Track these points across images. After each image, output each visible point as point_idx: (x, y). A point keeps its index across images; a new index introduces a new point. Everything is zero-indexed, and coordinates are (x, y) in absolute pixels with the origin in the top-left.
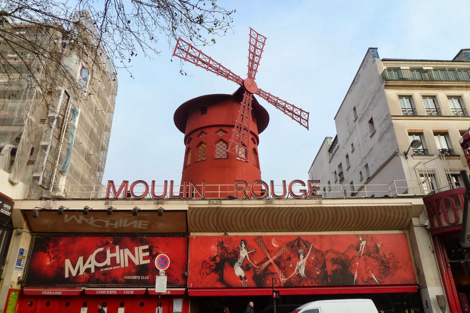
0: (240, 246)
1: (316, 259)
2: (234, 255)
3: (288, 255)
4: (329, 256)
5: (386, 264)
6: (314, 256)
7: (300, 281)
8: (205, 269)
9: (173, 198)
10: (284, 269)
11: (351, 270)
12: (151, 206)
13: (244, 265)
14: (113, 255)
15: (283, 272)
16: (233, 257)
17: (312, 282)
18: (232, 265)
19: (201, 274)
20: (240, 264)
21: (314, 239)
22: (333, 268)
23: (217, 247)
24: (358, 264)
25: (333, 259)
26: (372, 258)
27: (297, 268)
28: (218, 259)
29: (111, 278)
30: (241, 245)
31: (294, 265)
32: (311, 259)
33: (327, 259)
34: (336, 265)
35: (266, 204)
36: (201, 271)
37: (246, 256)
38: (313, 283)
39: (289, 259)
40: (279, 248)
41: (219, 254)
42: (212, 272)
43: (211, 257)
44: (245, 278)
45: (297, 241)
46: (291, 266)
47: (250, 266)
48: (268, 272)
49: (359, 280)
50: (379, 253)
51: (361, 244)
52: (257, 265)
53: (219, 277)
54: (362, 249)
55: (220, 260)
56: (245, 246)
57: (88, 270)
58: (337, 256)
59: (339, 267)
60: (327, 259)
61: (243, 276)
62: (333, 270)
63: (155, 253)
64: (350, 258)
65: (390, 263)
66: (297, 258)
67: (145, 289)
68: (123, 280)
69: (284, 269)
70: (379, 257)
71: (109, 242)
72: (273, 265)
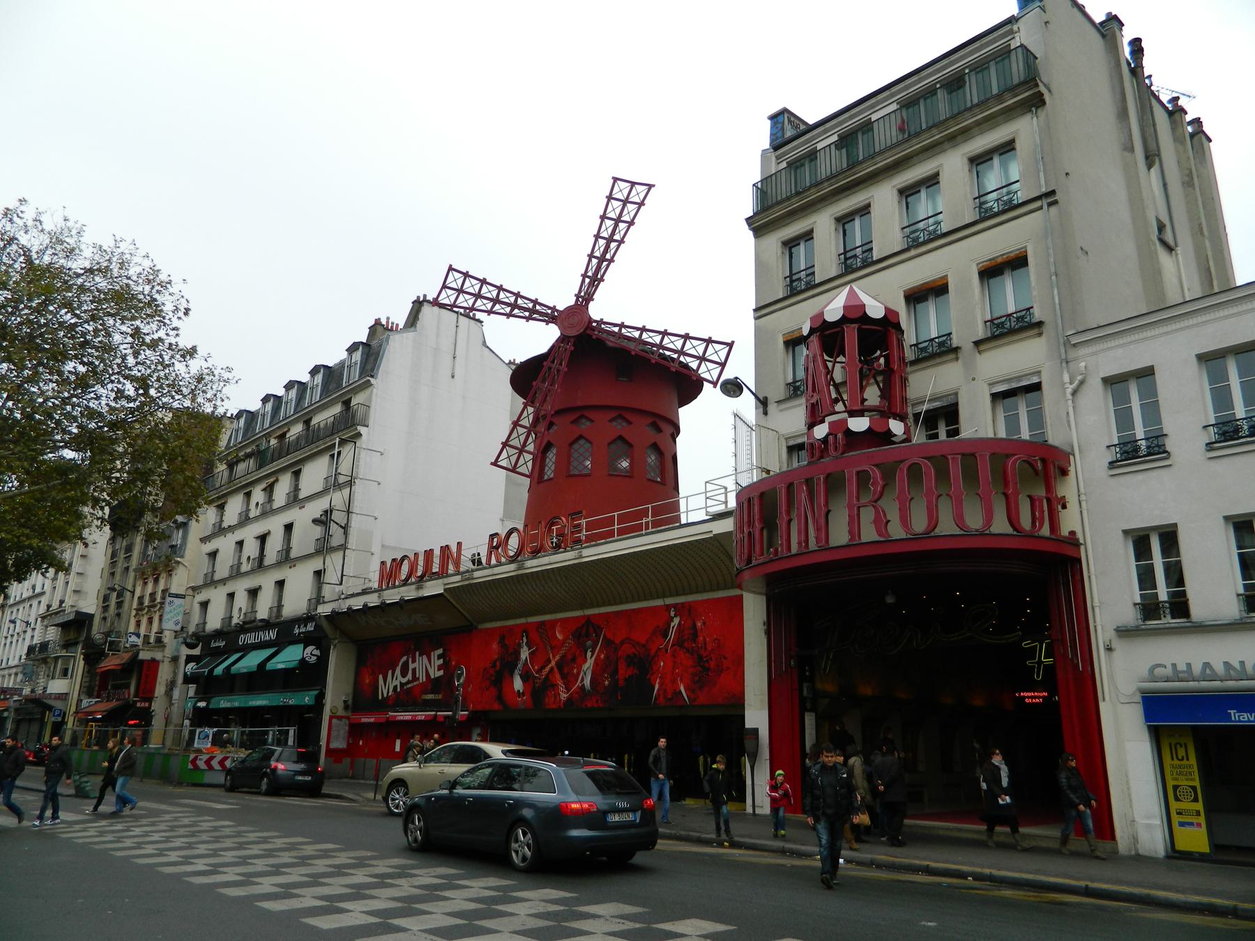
1: (607, 657)
15: (564, 683)
24: (662, 664)
27: (582, 673)
35: (519, 569)
39: (574, 660)
40: (564, 642)
44: (523, 694)
46: (575, 671)
51: (672, 624)
54: (672, 635)
57: (395, 687)
59: (635, 671)
61: (521, 691)
64: (653, 653)
65: (711, 659)
67: (433, 713)
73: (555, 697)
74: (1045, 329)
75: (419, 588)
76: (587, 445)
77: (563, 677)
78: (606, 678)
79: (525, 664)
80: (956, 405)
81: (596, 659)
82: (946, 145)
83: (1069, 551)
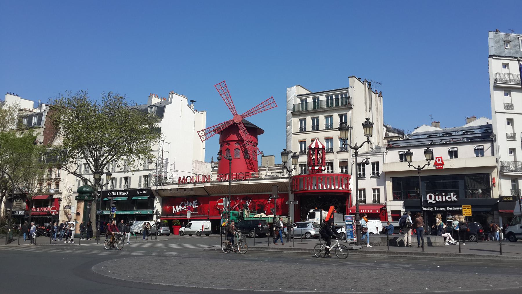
9: (200, 183)
12: (191, 186)
14: (186, 204)
57: (180, 210)
64: (265, 204)
74: (349, 152)
75: (194, 185)
80: (333, 162)
82: (335, 110)
83: (350, 192)
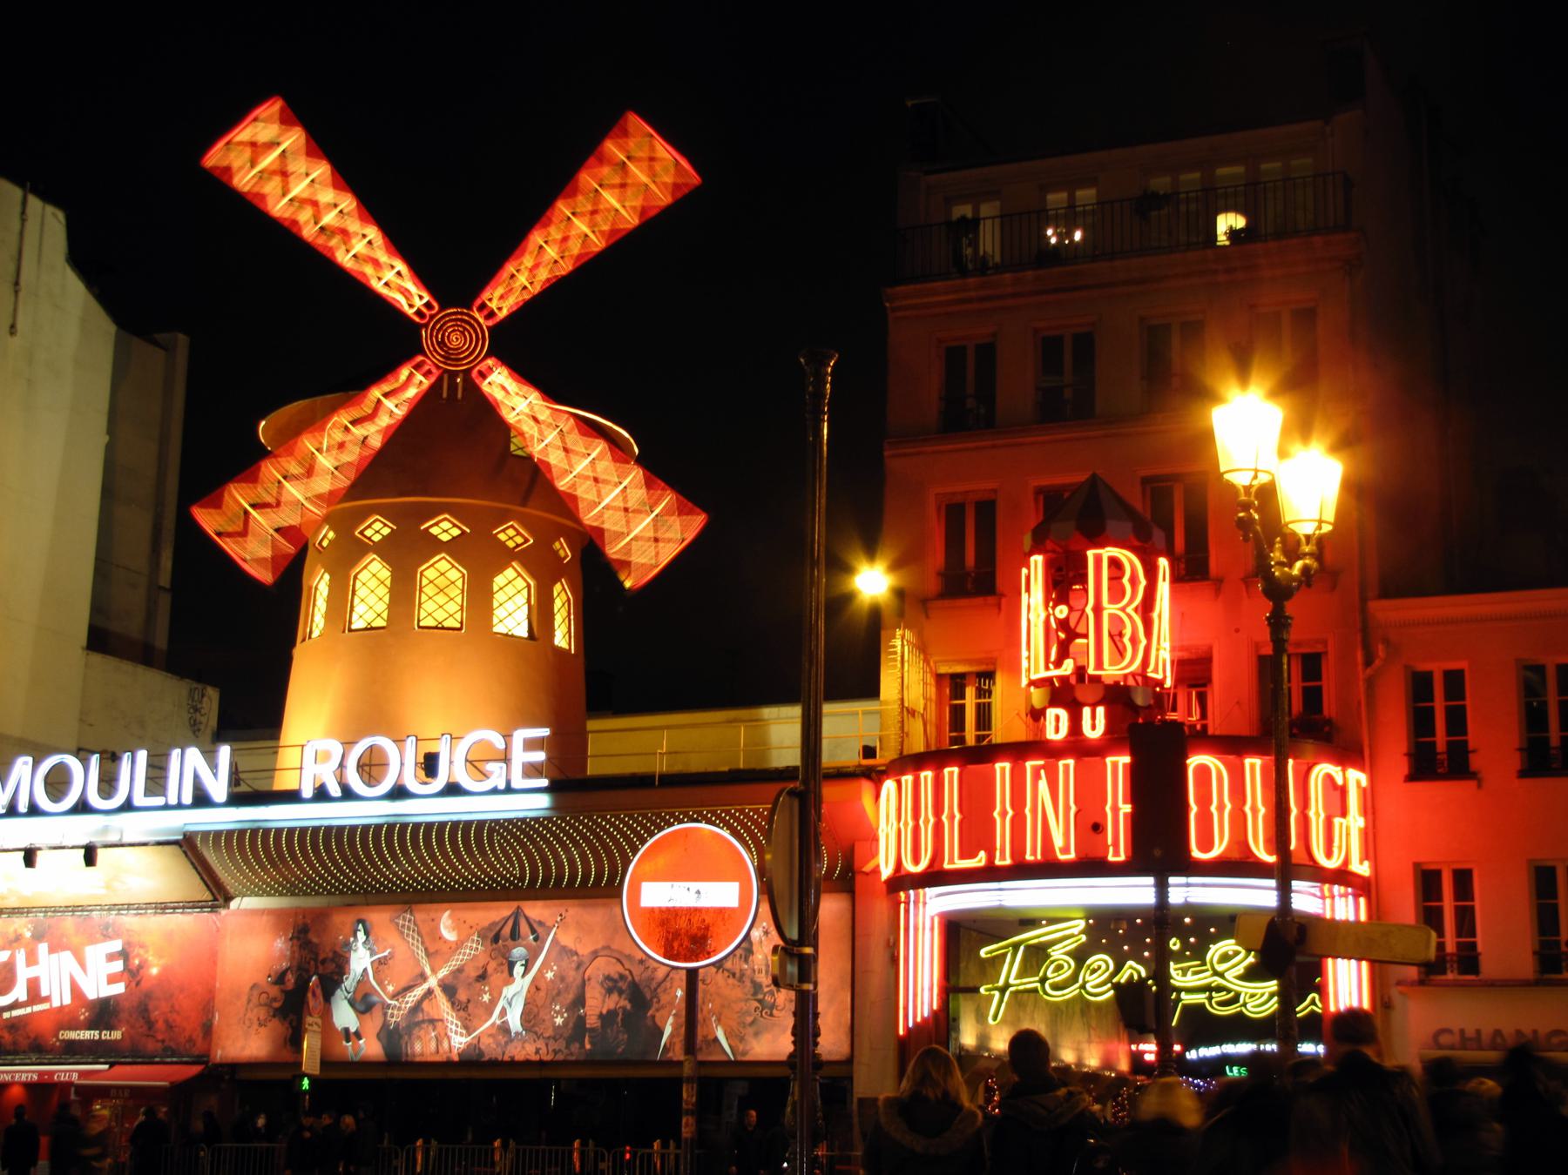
0: (352, 939)
1: (561, 977)
2: (334, 965)
3: (481, 965)
4: (598, 969)
5: (765, 996)
6: (555, 968)
7: (506, 1043)
8: (255, 1010)
10: (464, 1009)
11: (658, 1015)
13: (359, 997)
15: (459, 1018)
16: (332, 973)
17: (540, 1049)
18: (328, 995)
19: (244, 1023)
20: (349, 993)
21: (561, 915)
22: (603, 1007)
23: (290, 943)
25: (608, 978)
26: (726, 974)
27: (502, 1003)
28: (291, 979)
29: (29, 1037)
30: (355, 936)
31: (495, 995)
32: (545, 978)
33: (589, 979)
34: (615, 996)
36: (245, 1015)
37: (365, 970)
38: (541, 1052)
39: (482, 977)
40: (459, 945)
41: (295, 964)
42: (274, 1016)
43: (272, 974)
44: (358, 1035)
45: (510, 923)
46: (486, 998)
47: (375, 998)
48: (420, 1017)
49: (674, 1043)
50: (751, 958)
52: (394, 996)
53: (290, 1030)
55: (296, 983)
56: (365, 938)
58: (620, 968)
60: (589, 979)
61: (353, 1030)
62: (604, 1012)
63: (137, 962)
66: (506, 974)
68: (58, 1044)
69: (465, 1009)
70: (749, 972)
71: (20, 935)
72: (435, 997)
73: (438, 1041)
76: (454, 575)
77: (460, 1007)
78: (555, 1012)
79: (363, 980)
81: (534, 979)
